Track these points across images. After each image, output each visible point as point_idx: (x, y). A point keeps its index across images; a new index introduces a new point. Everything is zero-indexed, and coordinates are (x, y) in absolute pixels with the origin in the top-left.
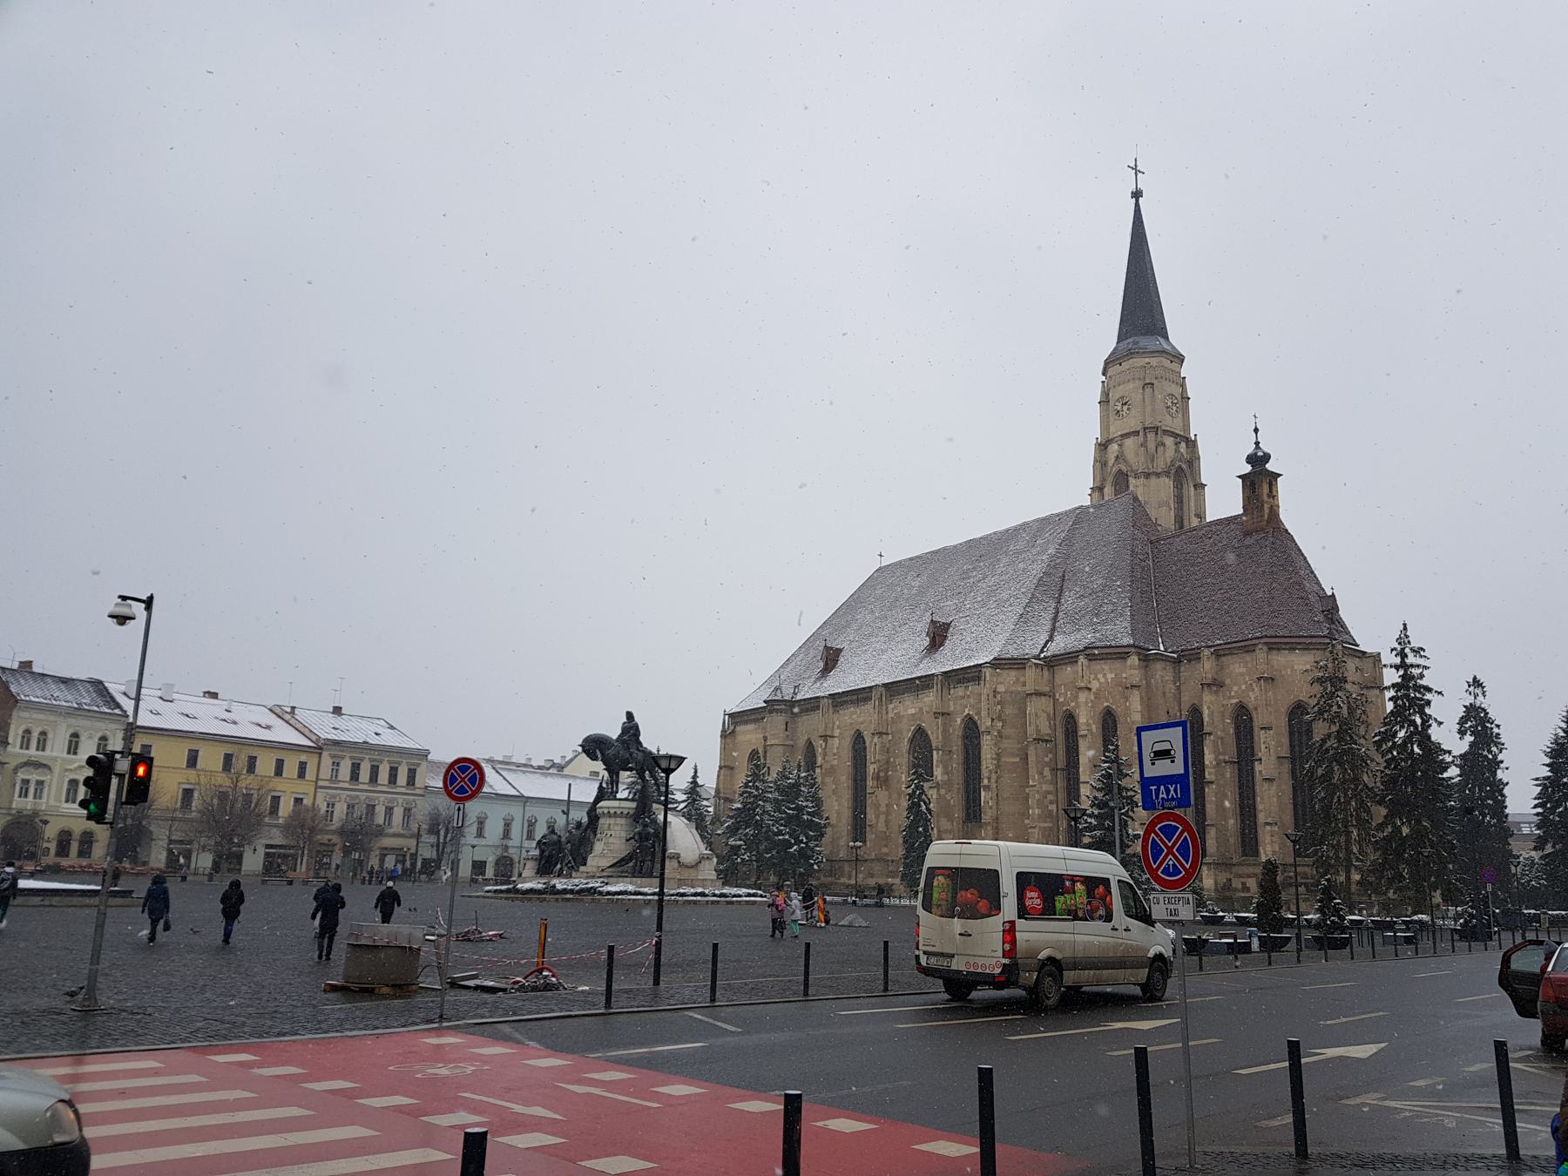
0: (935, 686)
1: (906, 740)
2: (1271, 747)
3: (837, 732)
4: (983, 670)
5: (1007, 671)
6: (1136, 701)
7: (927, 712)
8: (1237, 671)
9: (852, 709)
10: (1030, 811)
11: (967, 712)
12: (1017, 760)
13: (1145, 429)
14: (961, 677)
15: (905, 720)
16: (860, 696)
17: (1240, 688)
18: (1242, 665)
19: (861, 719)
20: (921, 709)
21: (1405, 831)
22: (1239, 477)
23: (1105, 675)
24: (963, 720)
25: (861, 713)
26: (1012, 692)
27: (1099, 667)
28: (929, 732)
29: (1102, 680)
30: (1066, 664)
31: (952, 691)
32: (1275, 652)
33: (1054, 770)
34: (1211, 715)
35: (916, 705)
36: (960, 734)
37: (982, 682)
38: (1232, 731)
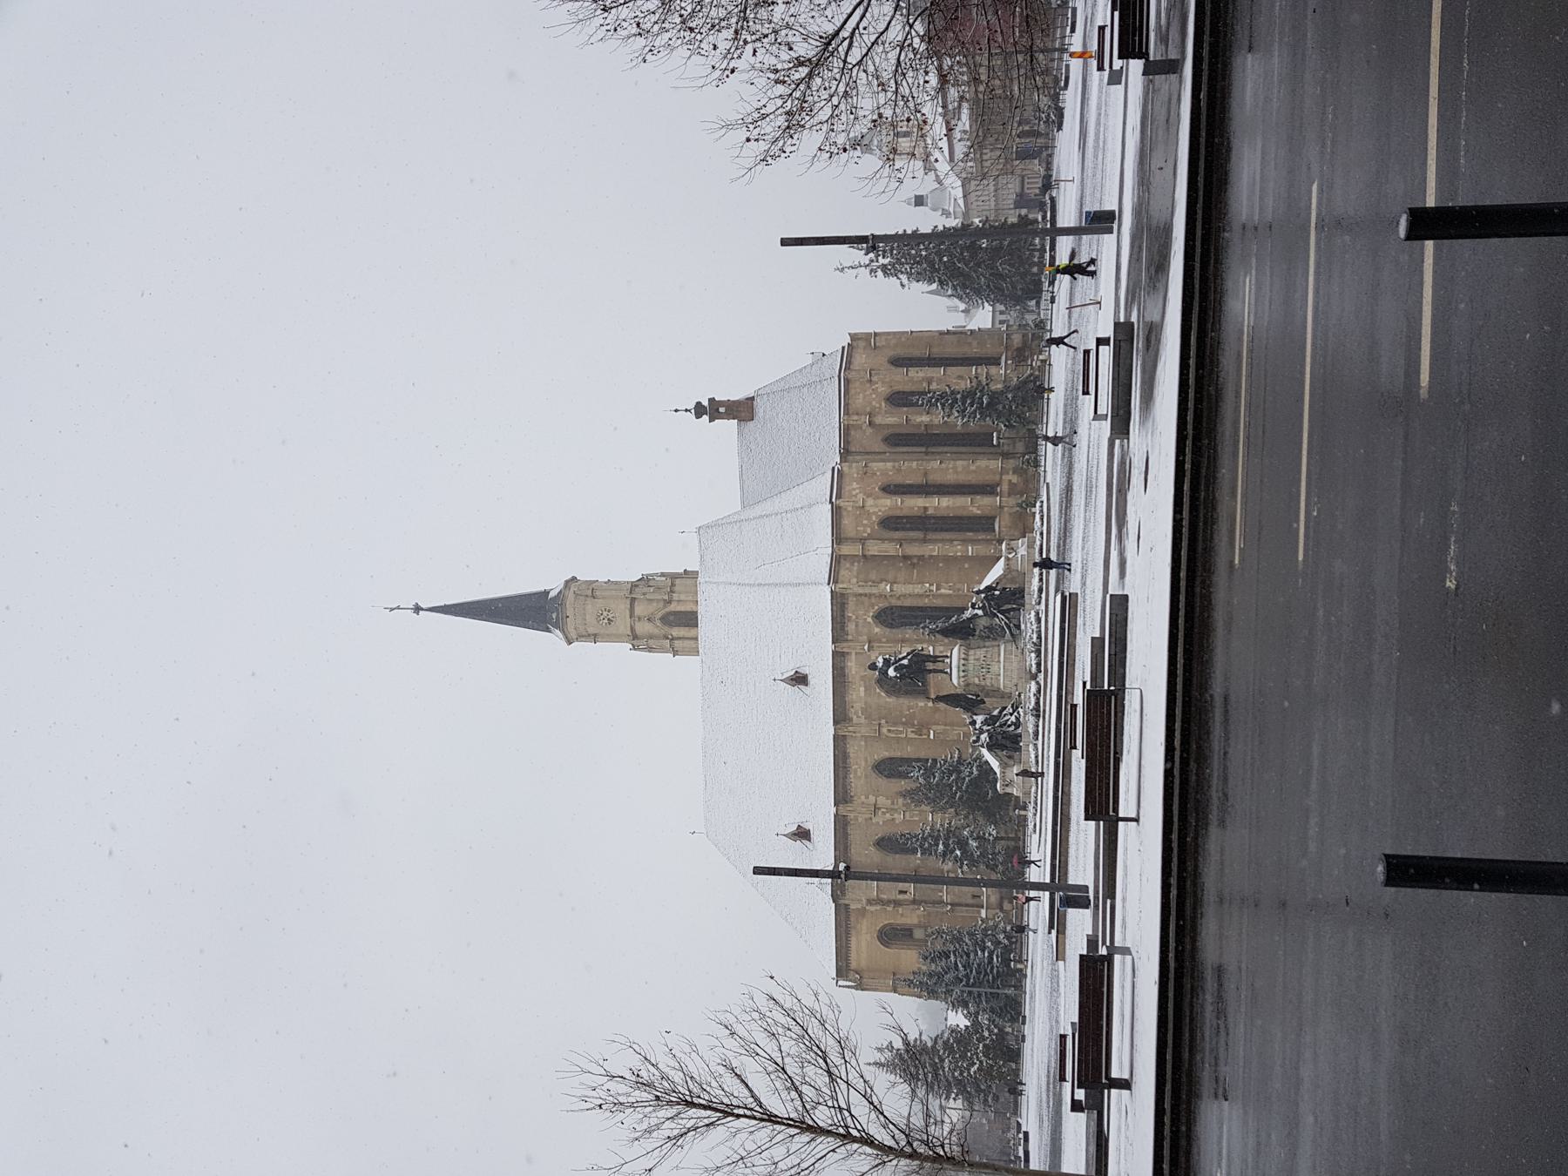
0: (845, 650)
1: (888, 700)
2: (911, 468)
3: (872, 799)
4: (837, 590)
5: (840, 577)
6: (875, 466)
8: (861, 401)
9: (851, 776)
10: (959, 554)
11: (870, 620)
12: (915, 571)
14: (839, 625)
16: (841, 765)
17: (874, 399)
19: (863, 763)
20: (863, 678)
21: (984, 245)
22: (710, 422)
23: (854, 489)
24: (877, 626)
26: (858, 574)
27: (847, 493)
29: (857, 491)
30: (840, 525)
31: (850, 637)
32: (851, 367)
33: (925, 541)
34: (893, 417)
36: (888, 630)
37: (848, 591)
38: (905, 409)
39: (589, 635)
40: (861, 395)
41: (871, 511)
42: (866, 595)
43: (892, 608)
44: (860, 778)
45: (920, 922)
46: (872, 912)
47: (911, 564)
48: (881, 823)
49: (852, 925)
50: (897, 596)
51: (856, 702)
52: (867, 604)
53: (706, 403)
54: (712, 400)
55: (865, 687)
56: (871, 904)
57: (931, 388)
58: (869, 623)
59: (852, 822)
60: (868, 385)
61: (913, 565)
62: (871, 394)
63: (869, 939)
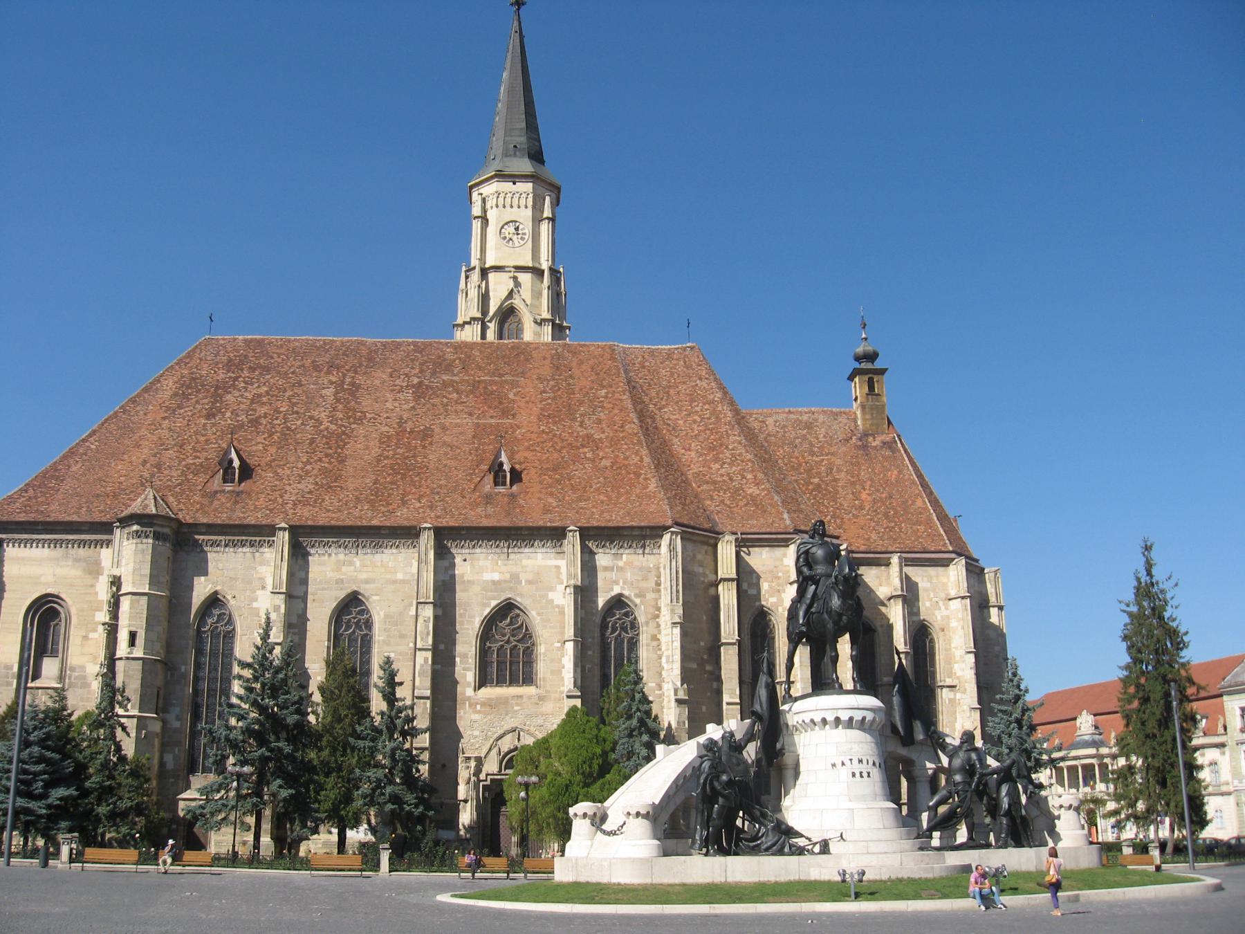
7: (530, 582)
11: (617, 590)
13: (550, 269)
15: (476, 589)
18: (925, 579)
19: (364, 576)
20: (515, 578)
25: (363, 566)
28: (533, 614)
35: (504, 569)
39: (485, 211)
40: (928, 585)
41: (783, 595)
42: (658, 584)
43: (634, 625)
44: (338, 570)
45: (73, 669)
46: (92, 586)
47: (702, 658)
48: (255, 605)
49: (71, 551)
50: (658, 636)
51: (472, 566)
52: (644, 585)
53: (878, 364)
54: (882, 372)
55: (499, 582)
56: (113, 583)
57: (944, 690)
58: (613, 590)
59: (257, 554)
60: (943, 595)
61: (702, 664)
62: (931, 600)
63: (43, 579)
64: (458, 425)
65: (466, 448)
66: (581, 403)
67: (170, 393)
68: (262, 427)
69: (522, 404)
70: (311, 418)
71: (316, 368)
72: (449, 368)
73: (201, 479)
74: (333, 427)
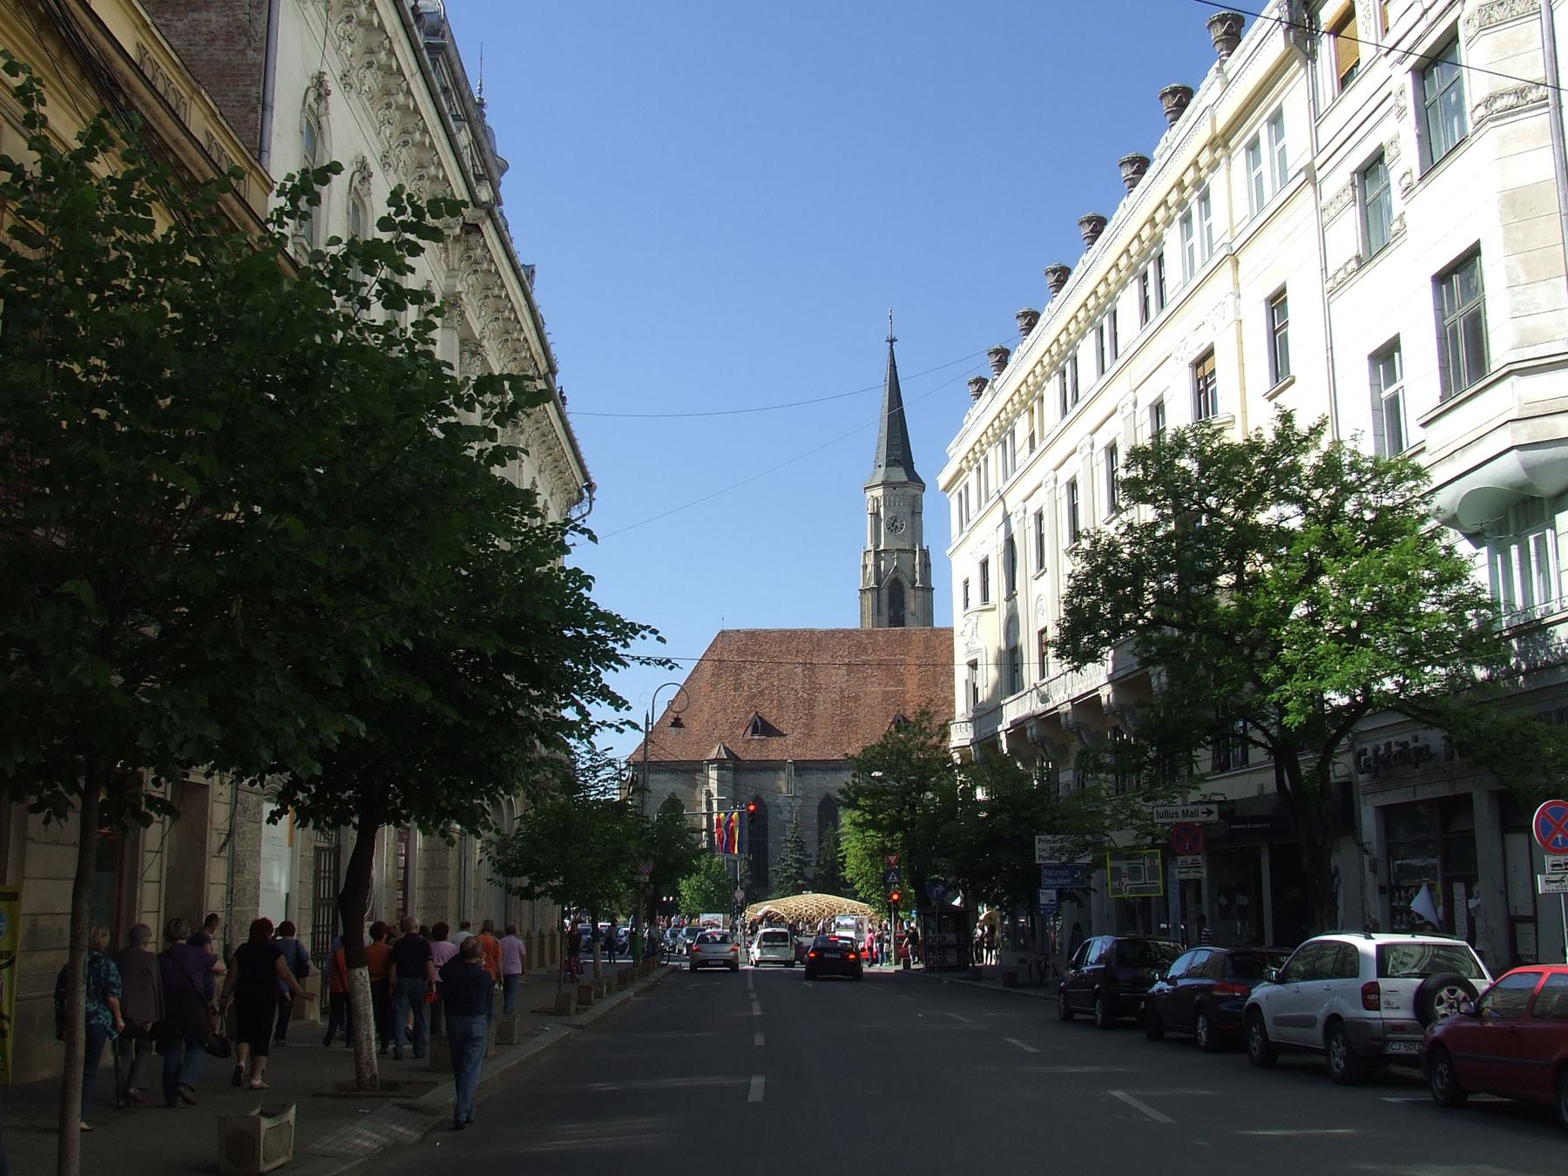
13: (921, 550)
64: (873, 692)
65: (879, 707)
66: (942, 674)
67: (710, 673)
68: (766, 697)
69: (908, 676)
70: (792, 689)
71: (789, 652)
72: (865, 650)
73: (742, 731)
74: (805, 695)
